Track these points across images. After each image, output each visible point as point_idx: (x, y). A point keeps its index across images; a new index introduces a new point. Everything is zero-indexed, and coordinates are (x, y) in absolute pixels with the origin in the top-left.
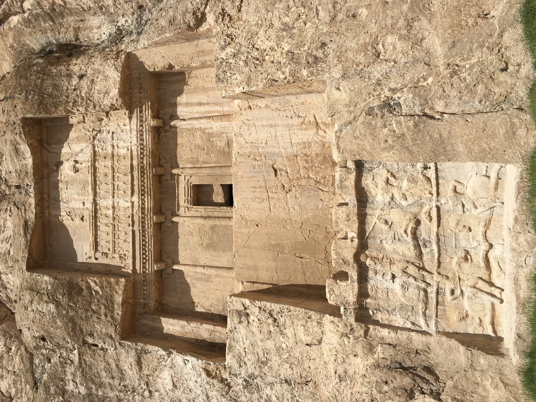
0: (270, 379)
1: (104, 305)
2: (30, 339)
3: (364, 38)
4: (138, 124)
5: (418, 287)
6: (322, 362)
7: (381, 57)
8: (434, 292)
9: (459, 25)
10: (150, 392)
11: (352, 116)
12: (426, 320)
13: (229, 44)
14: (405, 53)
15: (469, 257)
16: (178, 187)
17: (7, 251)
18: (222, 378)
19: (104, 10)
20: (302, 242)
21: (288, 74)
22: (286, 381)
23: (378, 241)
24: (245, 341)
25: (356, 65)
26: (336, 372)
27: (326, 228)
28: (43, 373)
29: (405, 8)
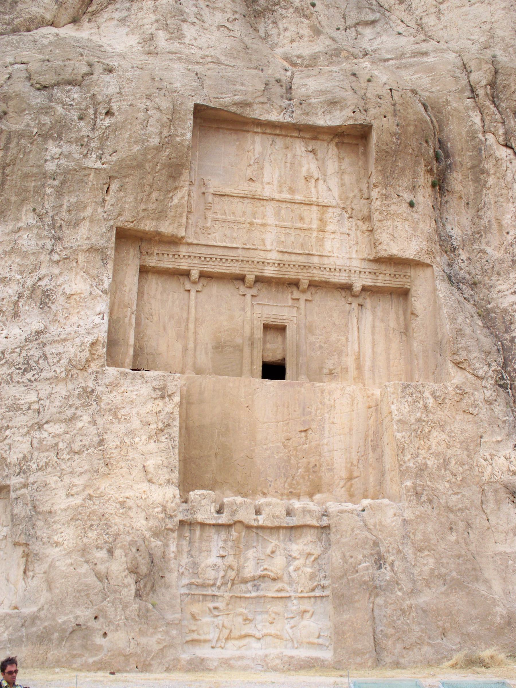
0: (100, 421)
1: (156, 208)
3: (434, 539)
5: (216, 579)
7: (419, 553)
10: (58, 262)
11: (372, 527)
13: (436, 400)
15: (248, 622)
19: (477, 236)
22: (102, 441)
23: (255, 544)
24: (135, 393)
26: (127, 498)
28: (64, 105)
29: (454, 574)
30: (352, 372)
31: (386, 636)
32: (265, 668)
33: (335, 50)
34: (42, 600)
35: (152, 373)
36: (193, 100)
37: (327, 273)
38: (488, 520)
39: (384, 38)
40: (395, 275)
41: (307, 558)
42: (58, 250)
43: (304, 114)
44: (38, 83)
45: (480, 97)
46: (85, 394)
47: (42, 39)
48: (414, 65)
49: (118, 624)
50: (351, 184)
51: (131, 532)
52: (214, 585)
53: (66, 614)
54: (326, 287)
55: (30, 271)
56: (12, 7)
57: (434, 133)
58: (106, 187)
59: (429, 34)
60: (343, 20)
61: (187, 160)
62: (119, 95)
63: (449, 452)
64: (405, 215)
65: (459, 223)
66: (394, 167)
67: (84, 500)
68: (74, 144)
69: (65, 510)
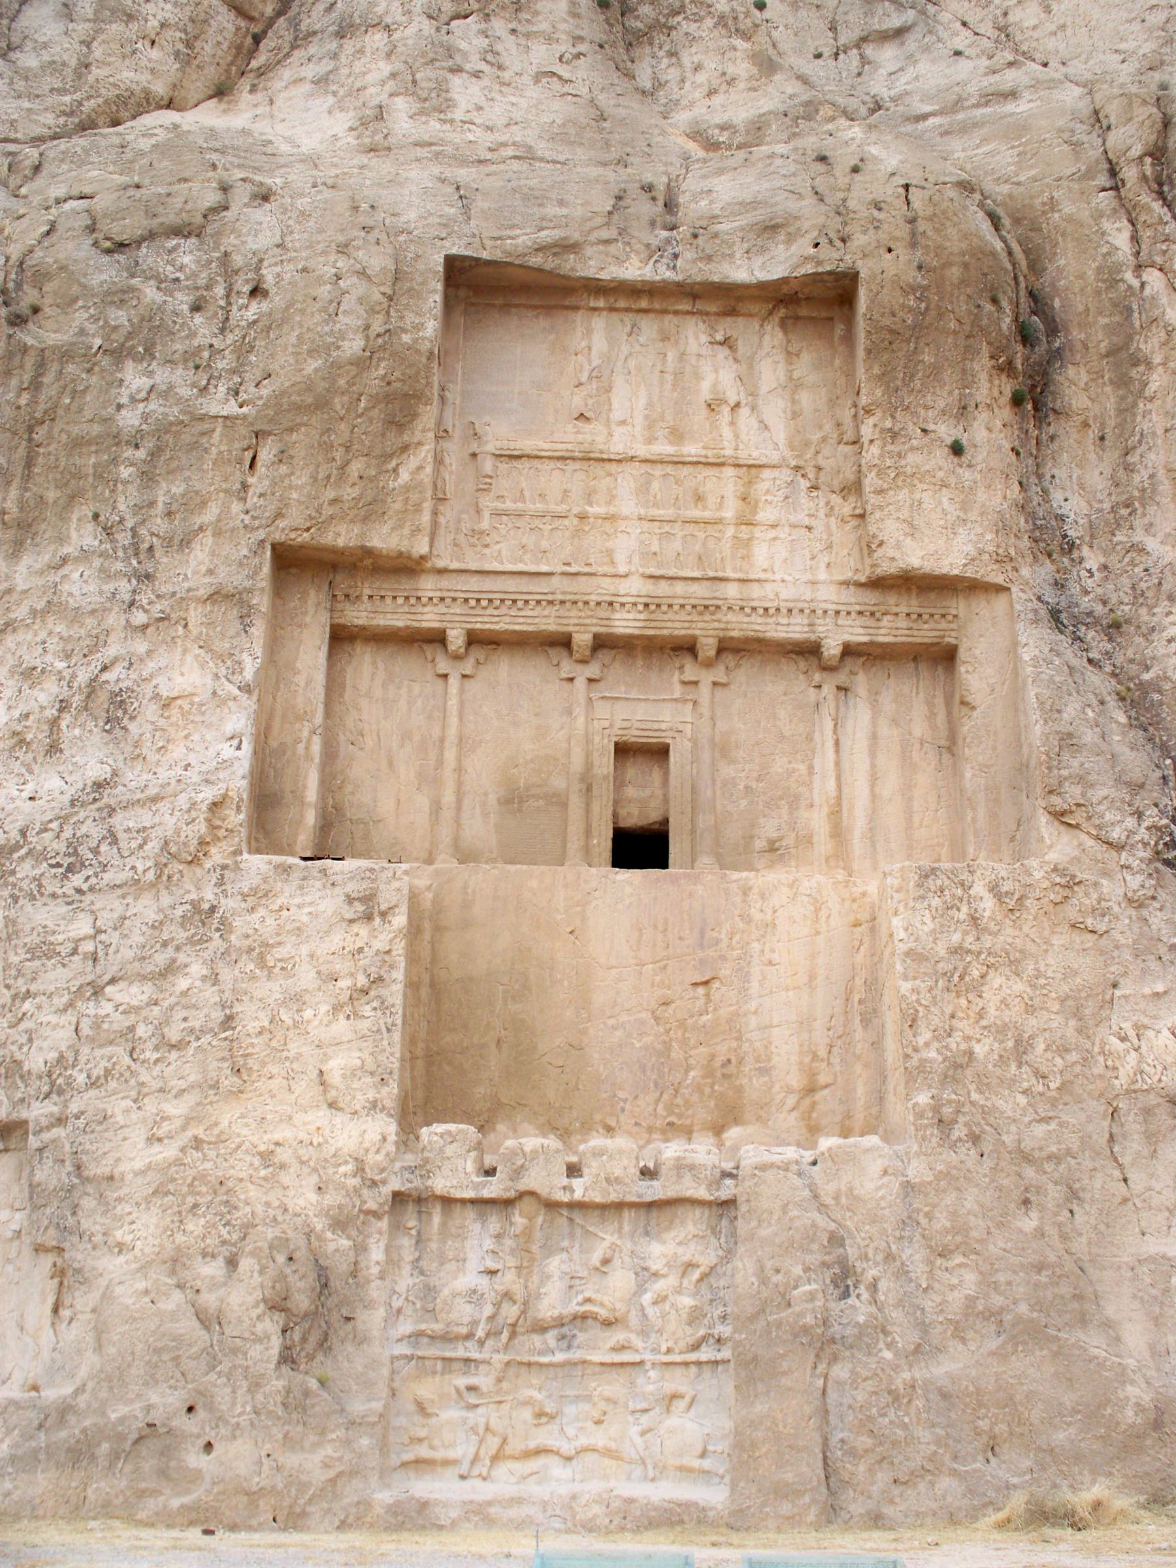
0: (227, 975)
1: (361, 496)
5: (475, 1323)
7: (939, 1261)
10: (145, 627)
11: (829, 1201)
13: (1001, 902)
14: (941, 1308)
15: (544, 1420)
17: (458, 59)
19: (1124, 512)
21: (924, 1054)
22: (230, 1018)
23: (565, 1244)
24: (306, 910)
26: (277, 1144)
28: (160, 280)
29: (1023, 1308)
30: (823, 844)
31: (852, 1453)
32: (569, 1524)
33: (808, 103)
34: (83, 1372)
35: (349, 864)
36: (443, 247)
37: (760, 620)
38: (1125, 1180)
39: (923, 67)
40: (920, 615)
41: (684, 1274)
42: (145, 601)
43: (701, 259)
44: (107, 239)
45: (1128, 186)
46: (197, 917)
47: (141, 140)
48: (983, 124)
49: (238, 1424)
50: (816, 410)
51: (280, 1219)
52: (469, 1336)
53: (132, 1401)
54: (760, 652)
55: (85, 651)
56: (79, 76)
57: (1015, 278)
58: (248, 455)
59: (1024, 48)
60: (830, 34)
61: (428, 384)
62: (279, 251)
64: (940, 474)
65: (1082, 486)
66: (912, 364)
67: (183, 1150)
68: (181, 366)
69: (142, 1173)
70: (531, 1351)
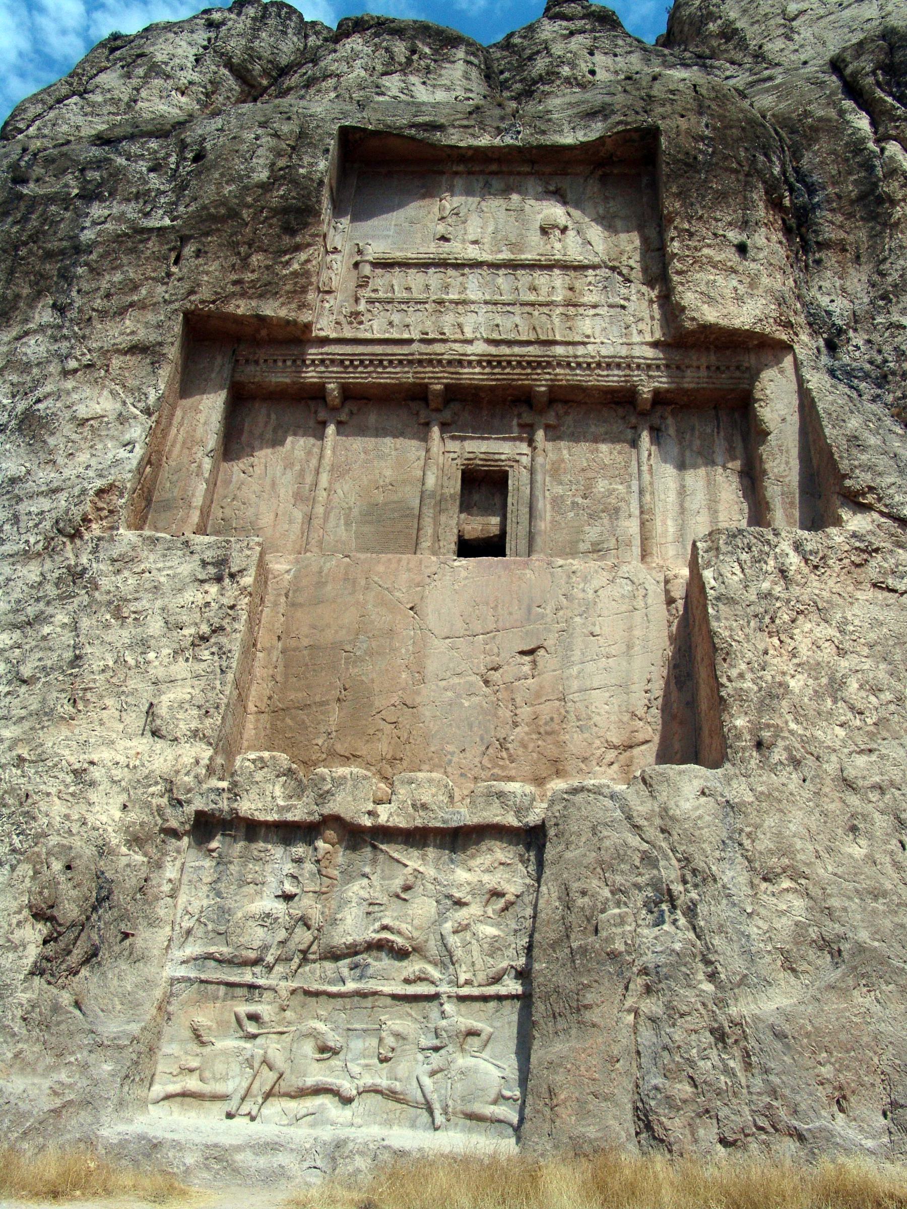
0: (85, 623)
1: (258, 280)
2: (200, 132)
3: (805, 850)
4: (642, 361)
5: (265, 948)
6: (114, 736)
7: (764, 885)
8: (255, 980)
9: (820, 1048)
10: (75, 371)
12: (196, 959)
13: (806, 561)
15: (325, 1056)
16: (504, 439)
17: (383, 89)
18: (90, 521)
19: (881, 303)
20: (371, 705)
22: (78, 657)
23: (367, 870)
24: (165, 573)
25: (750, 833)
26: (92, 763)
27: (401, 759)
29: (864, 935)
43: (537, 133)
63: (843, 664)
70: (323, 979)
